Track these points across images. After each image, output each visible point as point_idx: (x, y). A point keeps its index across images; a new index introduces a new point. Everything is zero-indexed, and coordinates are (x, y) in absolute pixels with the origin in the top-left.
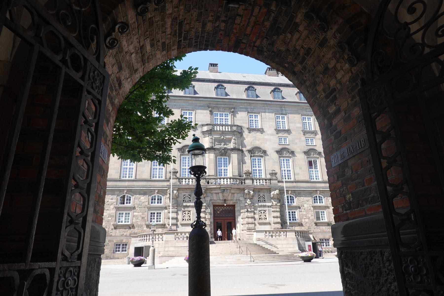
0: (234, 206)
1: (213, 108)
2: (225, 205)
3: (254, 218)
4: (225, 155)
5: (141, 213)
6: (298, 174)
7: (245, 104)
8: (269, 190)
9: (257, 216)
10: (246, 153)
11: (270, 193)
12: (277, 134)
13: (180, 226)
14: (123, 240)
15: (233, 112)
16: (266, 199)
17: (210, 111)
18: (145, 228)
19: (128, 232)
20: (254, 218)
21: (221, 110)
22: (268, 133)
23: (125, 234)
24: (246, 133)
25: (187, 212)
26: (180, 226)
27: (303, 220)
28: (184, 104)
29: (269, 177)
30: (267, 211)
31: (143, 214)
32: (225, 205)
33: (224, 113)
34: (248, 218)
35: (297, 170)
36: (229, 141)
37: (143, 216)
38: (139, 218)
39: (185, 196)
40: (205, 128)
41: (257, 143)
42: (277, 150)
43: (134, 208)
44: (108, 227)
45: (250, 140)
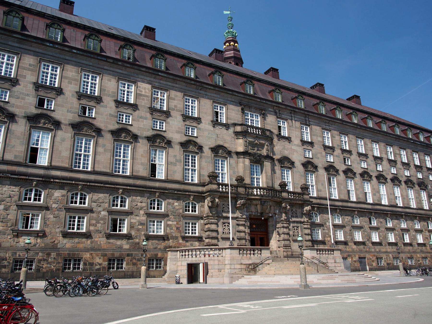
0: (266, 220)
1: (245, 106)
2: (263, 219)
3: (288, 234)
4: (258, 163)
5: (175, 223)
6: (321, 191)
7: (275, 107)
8: (302, 206)
9: (291, 233)
10: (276, 162)
11: (303, 208)
12: (303, 145)
13: (220, 240)
14: (158, 254)
15: (264, 114)
16: (298, 215)
17: (242, 109)
18: (181, 241)
19: (163, 244)
20: (288, 234)
21: (253, 109)
22: (295, 143)
23: (159, 247)
24: (275, 140)
25: (226, 224)
26: (220, 240)
27: (326, 239)
28: (215, 95)
29: (299, 190)
30: (299, 228)
31: (177, 224)
32: (263, 219)
33: (254, 114)
34: (284, 234)
35: (320, 187)
36: (262, 146)
37: (178, 226)
38: (173, 229)
39: (224, 206)
40: (238, 129)
41: (286, 153)
42: (303, 162)
43: (167, 216)
44: (138, 237)
45: (280, 149)
